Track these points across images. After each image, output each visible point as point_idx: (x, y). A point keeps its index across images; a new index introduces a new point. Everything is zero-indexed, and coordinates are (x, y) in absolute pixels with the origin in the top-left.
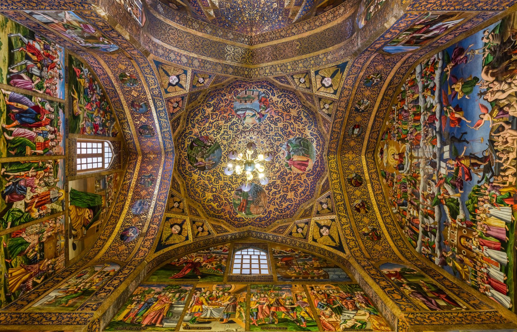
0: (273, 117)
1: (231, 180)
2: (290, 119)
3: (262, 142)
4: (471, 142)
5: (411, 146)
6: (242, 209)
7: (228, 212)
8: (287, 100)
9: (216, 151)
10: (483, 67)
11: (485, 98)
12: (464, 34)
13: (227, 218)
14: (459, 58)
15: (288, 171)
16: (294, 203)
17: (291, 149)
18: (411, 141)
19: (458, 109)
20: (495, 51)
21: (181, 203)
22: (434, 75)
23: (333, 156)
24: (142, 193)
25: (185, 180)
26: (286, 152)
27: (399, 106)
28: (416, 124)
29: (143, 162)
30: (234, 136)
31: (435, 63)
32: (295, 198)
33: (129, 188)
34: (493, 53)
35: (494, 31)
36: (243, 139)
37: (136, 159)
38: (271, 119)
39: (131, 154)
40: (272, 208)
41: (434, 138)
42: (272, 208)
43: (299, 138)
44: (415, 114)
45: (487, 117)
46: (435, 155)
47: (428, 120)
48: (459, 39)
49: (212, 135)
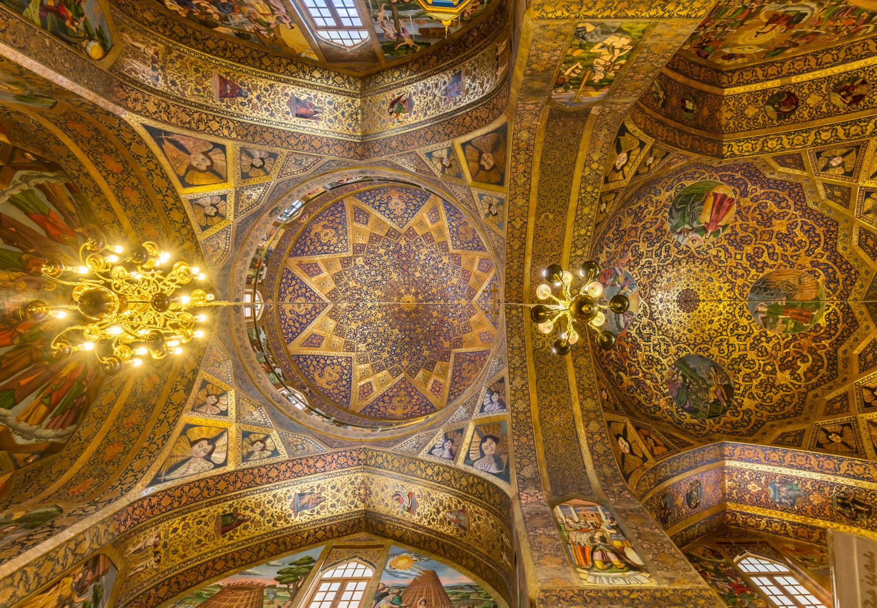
0: (630, 260)
1: (743, 337)
2: (636, 229)
3: (669, 280)
6: (806, 316)
7: (815, 341)
8: (607, 236)
9: (691, 366)
13: (831, 344)
15: (728, 231)
16: (799, 220)
17: (687, 226)
21: (828, 428)
23: (725, 148)
24: (815, 502)
25: (764, 423)
26: (692, 235)
29: (740, 501)
30: (660, 333)
32: (787, 218)
33: (807, 526)
36: (664, 317)
37: (734, 514)
38: (632, 264)
39: (725, 522)
40: (805, 261)
42: (805, 261)
43: (670, 213)
49: (664, 373)
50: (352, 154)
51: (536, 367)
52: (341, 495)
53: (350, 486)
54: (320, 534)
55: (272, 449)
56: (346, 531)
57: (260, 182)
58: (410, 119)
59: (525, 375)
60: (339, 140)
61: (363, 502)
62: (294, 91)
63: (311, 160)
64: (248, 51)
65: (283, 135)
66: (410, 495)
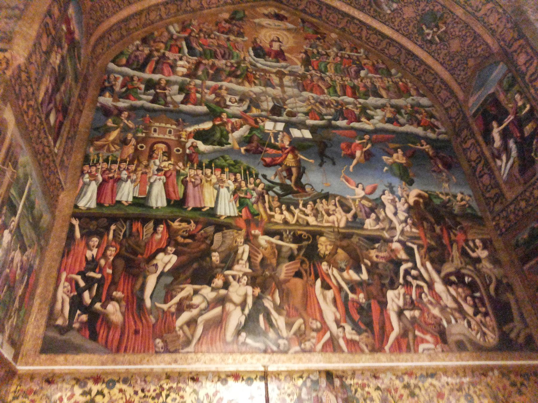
4: (322, 169)
5: (300, 76)
10: (426, 192)
11: (386, 192)
12: (469, 172)
14: (438, 162)
18: (309, 77)
19: (368, 155)
20: (446, 207)
22: (416, 124)
27: (366, 61)
28: (338, 89)
31: (433, 127)
34: (444, 205)
35: (470, 207)
41: (321, 117)
44: (354, 89)
45: (360, 193)
46: (292, 114)
47: (347, 109)
48: (465, 165)
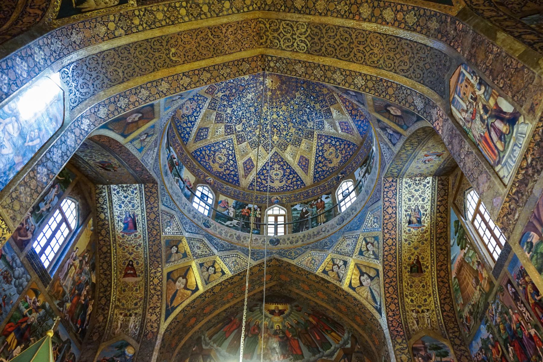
50: (154, 190)
51: (325, 56)
52: (417, 194)
53: (412, 187)
54: (442, 209)
55: (373, 239)
56: (445, 190)
57: (187, 245)
58: (116, 162)
59: (332, 69)
60: (146, 200)
61: (426, 177)
62: (119, 231)
63: (165, 217)
64: (102, 261)
65: (152, 239)
66: (426, 156)
